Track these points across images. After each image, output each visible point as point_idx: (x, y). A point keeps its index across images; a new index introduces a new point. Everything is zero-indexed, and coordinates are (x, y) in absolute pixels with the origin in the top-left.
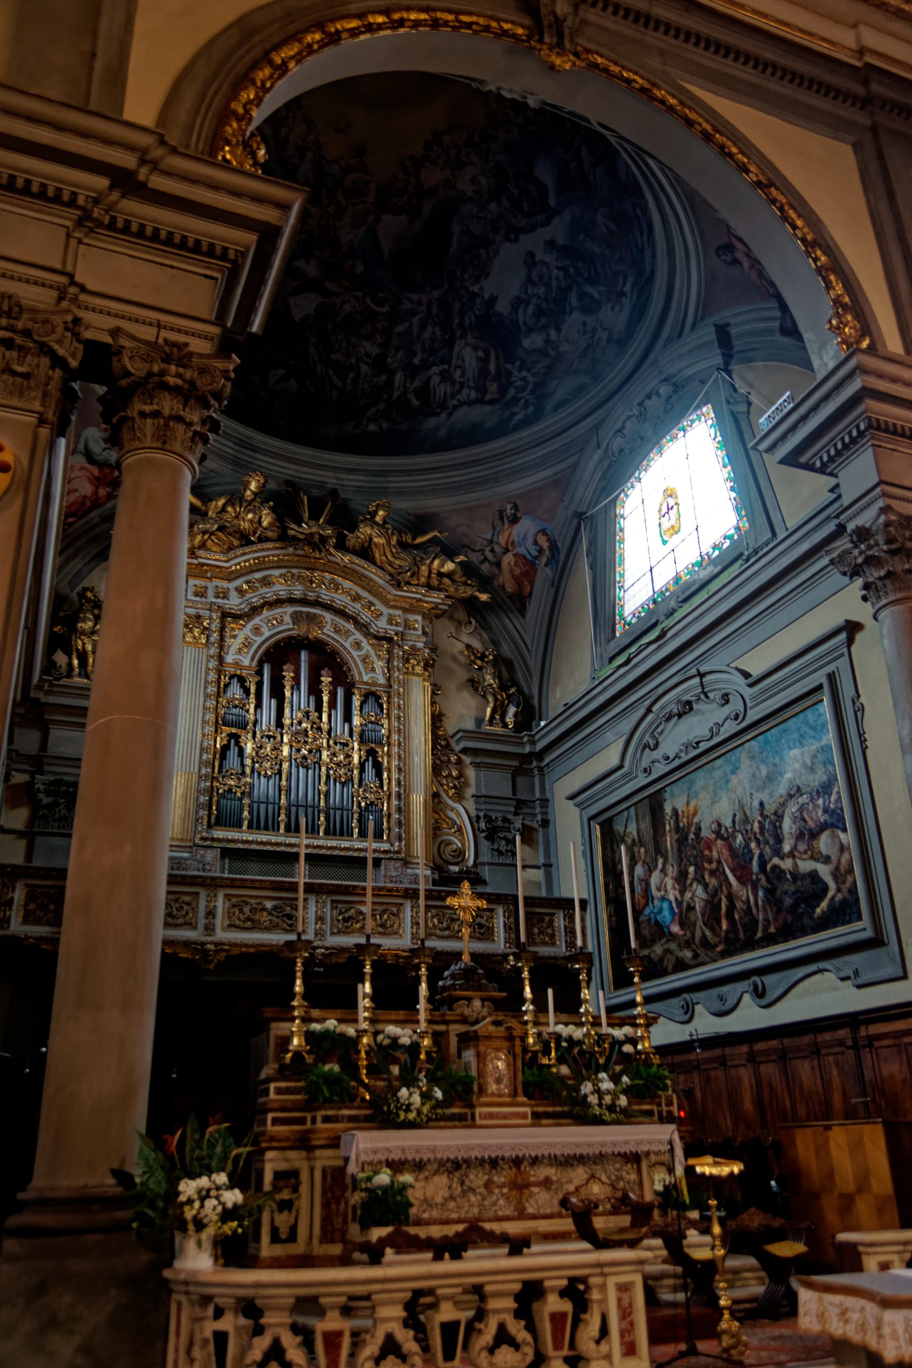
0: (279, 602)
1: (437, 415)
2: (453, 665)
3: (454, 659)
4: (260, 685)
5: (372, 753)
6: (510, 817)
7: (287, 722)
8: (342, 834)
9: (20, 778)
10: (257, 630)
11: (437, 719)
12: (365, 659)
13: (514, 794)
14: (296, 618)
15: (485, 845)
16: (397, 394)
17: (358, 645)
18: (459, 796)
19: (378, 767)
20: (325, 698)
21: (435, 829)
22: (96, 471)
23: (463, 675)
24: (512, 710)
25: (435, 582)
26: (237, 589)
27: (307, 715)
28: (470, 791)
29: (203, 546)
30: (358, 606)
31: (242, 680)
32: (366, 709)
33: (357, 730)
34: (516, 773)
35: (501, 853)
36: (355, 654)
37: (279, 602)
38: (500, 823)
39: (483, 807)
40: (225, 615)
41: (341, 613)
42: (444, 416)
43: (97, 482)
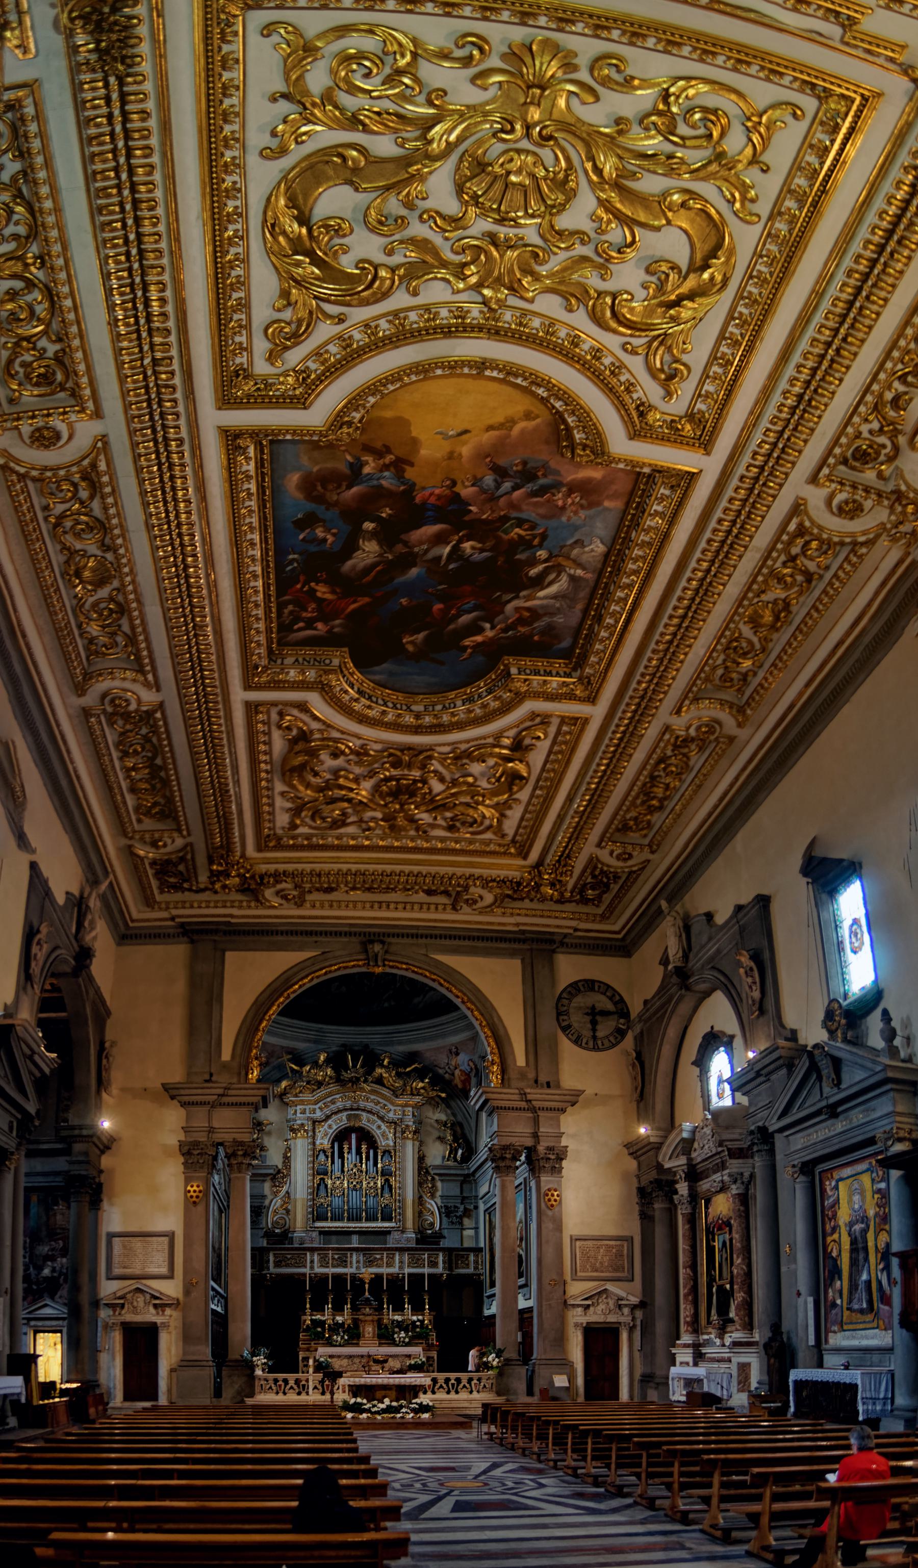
2: (430, 1129)
3: (432, 1126)
5: (387, 1181)
11: (421, 1159)
12: (384, 1135)
15: (445, 1219)
17: (379, 1127)
18: (433, 1196)
19: (390, 1187)
21: (419, 1214)
23: (436, 1134)
28: (439, 1193)
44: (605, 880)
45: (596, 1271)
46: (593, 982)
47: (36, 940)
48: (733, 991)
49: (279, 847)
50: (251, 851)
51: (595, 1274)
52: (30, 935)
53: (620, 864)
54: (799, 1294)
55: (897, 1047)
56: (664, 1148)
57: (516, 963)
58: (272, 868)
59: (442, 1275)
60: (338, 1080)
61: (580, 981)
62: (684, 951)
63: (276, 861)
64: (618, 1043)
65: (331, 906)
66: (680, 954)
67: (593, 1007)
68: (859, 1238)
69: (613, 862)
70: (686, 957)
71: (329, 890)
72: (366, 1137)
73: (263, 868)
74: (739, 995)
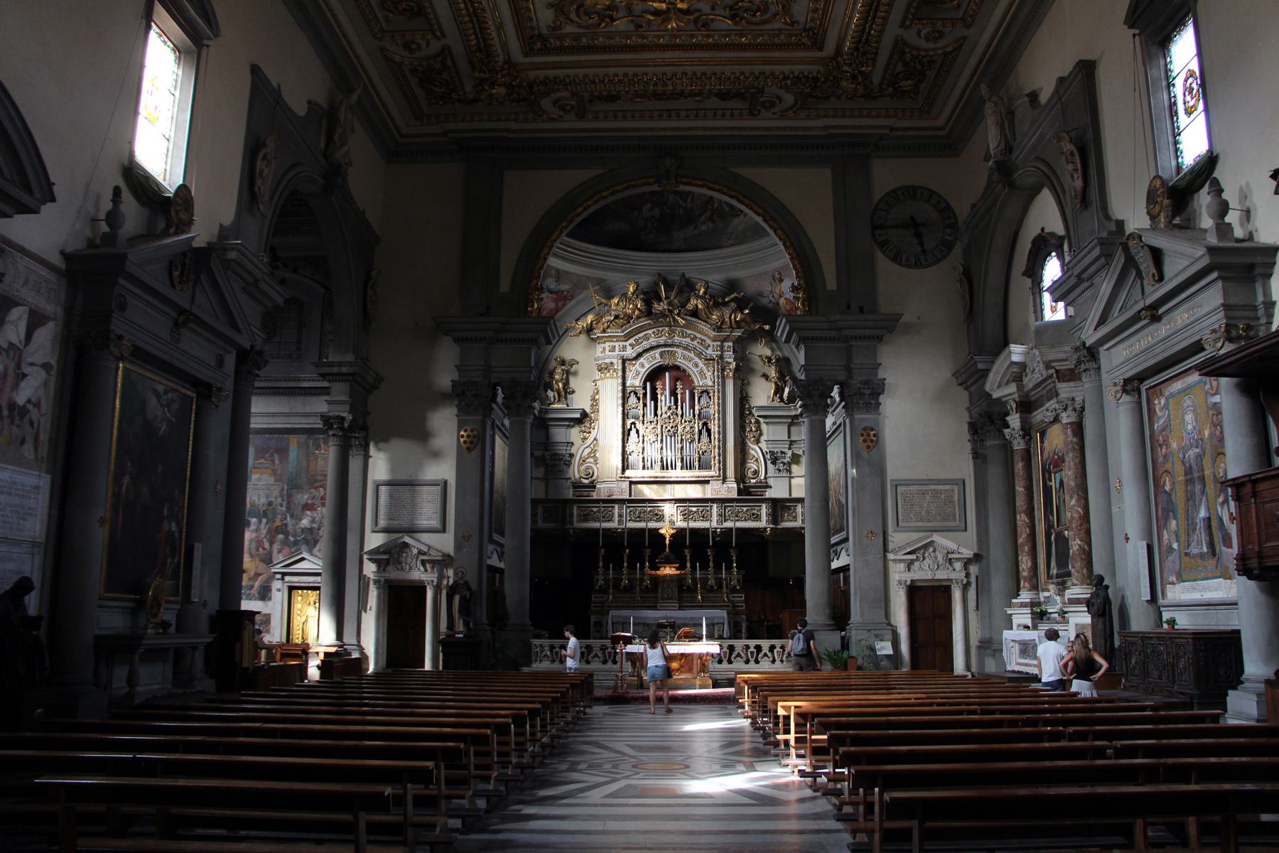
0: (652, 348)
1: (739, 215)
4: (645, 395)
5: (705, 424)
6: (786, 450)
7: (659, 412)
8: (690, 469)
9: (537, 453)
10: (643, 366)
13: (789, 437)
14: (661, 354)
15: (770, 466)
16: (716, 205)
17: (697, 366)
19: (709, 431)
20: (679, 396)
22: (555, 296)
24: (787, 390)
25: (734, 326)
26: (630, 345)
27: (669, 408)
28: (763, 438)
29: (608, 327)
30: (695, 343)
31: (636, 393)
32: (702, 399)
33: (697, 412)
34: (790, 426)
35: (780, 470)
36: (695, 370)
37: (652, 348)
38: (779, 455)
39: (770, 446)
40: (624, 361)
41: (686, 348)
42: (742, 217)
43: (556, 301)
44: (919, 67)
45: (921, 520)
46: (914, 188)
47: (261, 155)
48: (1055, 182)
49: (546, 50)
50: (517, 56)
51: (920, 524)
52: (253, 150)
53: (931, 45)
54: (1127, 539)
55: (1230, 224)
56: (991, 375)
57: (826, 173)
58: (542, 74)
59: (765, 529)
60: (649, 313)
61: (900, 188)
62: (1007, 142)
63: (546, 66)
64: (944, 257)
65: (616, 117)
66: (1003, 145)
67: (912, 219)
68: (1194, 467)
69: (923, 44)
70: (1009, 149)
71: (613, 98)
72: (680, 375)
73: (532, 74)
74: (1062, 186)
